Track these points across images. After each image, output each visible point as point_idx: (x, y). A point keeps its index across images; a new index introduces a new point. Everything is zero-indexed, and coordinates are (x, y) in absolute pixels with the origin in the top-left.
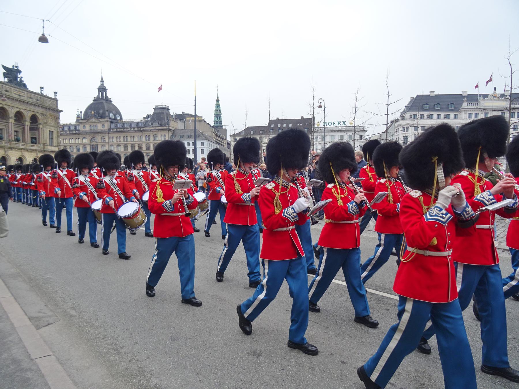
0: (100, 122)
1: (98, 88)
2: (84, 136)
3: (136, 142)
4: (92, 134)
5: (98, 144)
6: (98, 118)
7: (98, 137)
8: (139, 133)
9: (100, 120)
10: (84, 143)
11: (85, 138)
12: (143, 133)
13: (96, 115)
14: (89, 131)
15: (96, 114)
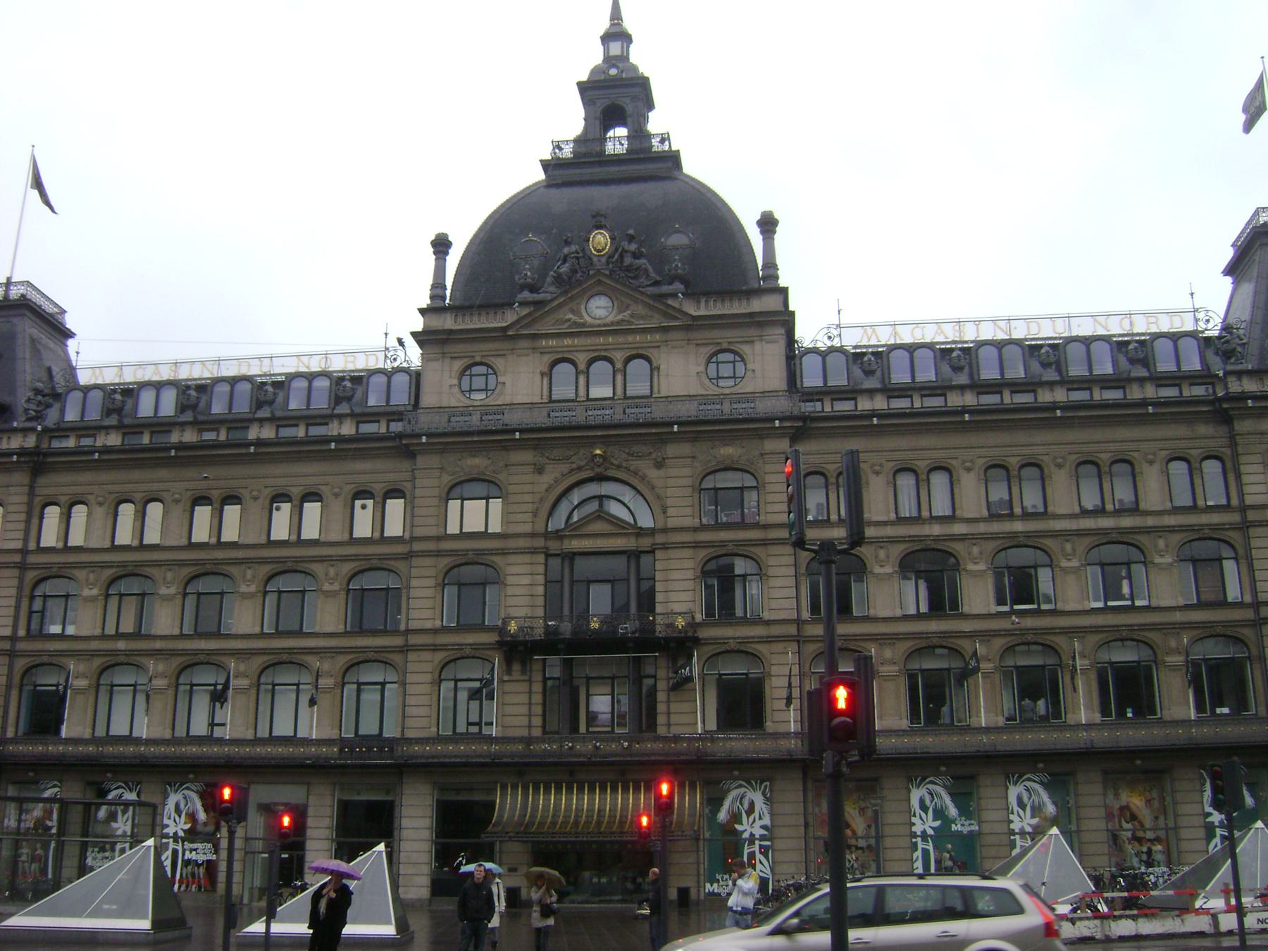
0: (694, 325)
1: (584, 78)
2: (476, 463)
3: (1150, 521)
4: (593, 442)
5: (645, 543)
6: (665, 289)
7: (653, 474)
8: (1180, 430)
9: (691, 309)
10: (463, 536)
11: (469, 489)
12: (1243, 426)
13: (628, 260)
14: (539, 418)
15: (636, 255)
